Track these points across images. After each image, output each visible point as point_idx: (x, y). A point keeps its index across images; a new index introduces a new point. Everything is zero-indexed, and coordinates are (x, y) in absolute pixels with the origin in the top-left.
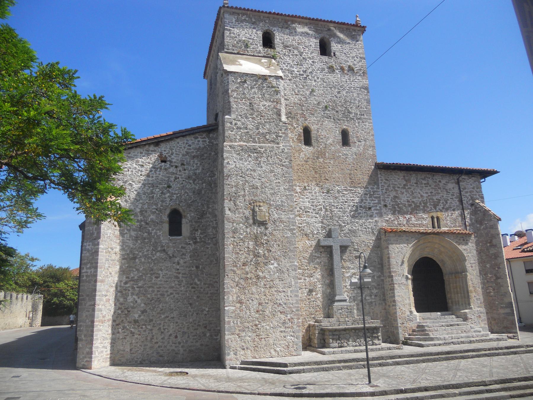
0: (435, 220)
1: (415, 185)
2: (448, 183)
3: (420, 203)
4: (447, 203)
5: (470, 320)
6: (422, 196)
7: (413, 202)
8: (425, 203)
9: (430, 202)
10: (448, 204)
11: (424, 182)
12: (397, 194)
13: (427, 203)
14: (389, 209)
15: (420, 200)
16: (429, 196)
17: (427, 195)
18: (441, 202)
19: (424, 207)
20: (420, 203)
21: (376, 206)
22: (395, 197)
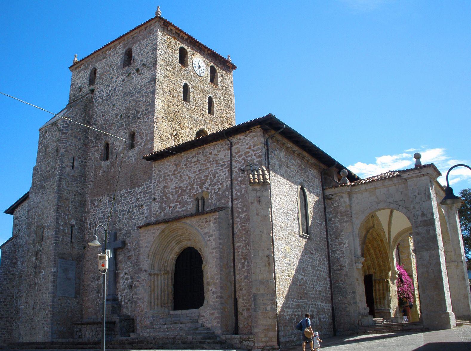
0: (200, 201)
1: (185, 167)
2: (220, 151)
3: (187, 187)
4: (215, 177)
5: (202, 318)
6: (189, 178)
7: (180, 187)
8: (192, 185)
9: (197, 182)
10: (217, 178)
11: (193, 160)
12: (166, 183)
13: (193, 184)
14: (158, 202)
15: (187, 183)
16: (197, 175)
17: (195, 175)
18: (209, 178)
19: (190, 189)
20: (187, 187)
21: (147, 202)
22: (165, 187)
